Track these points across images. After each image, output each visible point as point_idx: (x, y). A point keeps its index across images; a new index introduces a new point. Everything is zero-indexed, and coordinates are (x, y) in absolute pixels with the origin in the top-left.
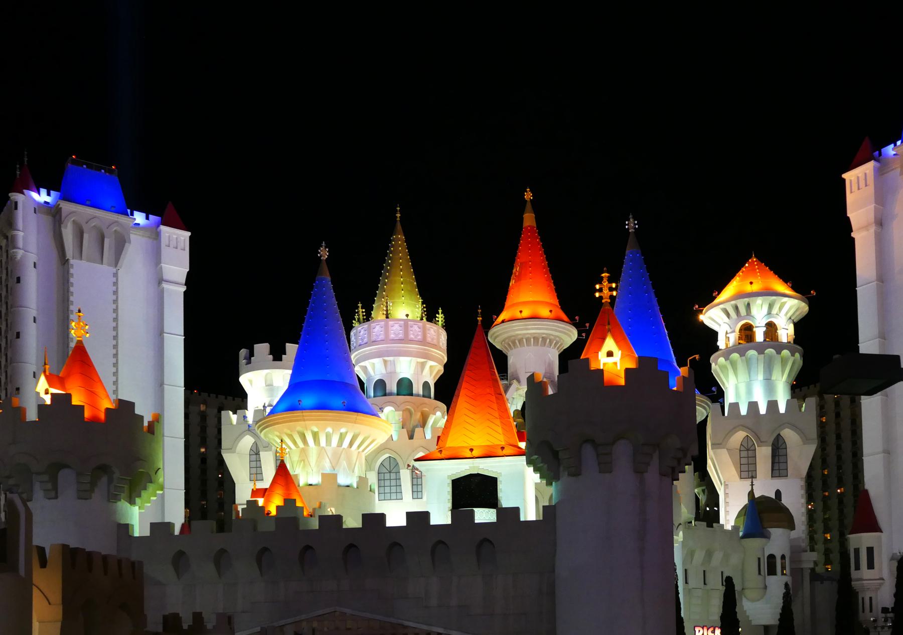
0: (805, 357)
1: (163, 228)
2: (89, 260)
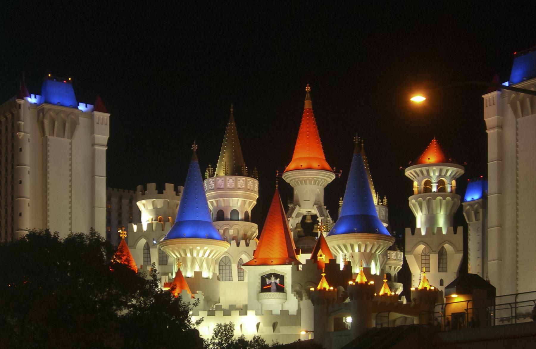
1: (96, 113)
2: (58, 136)
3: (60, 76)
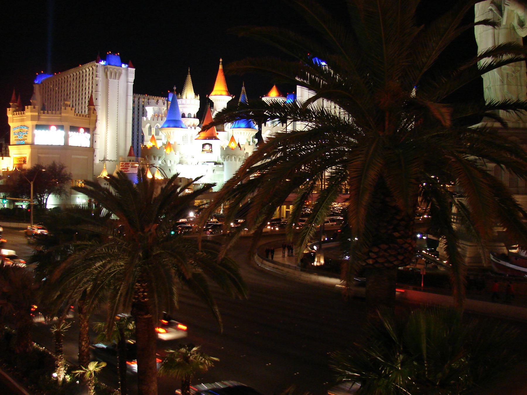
3: (114, 52)
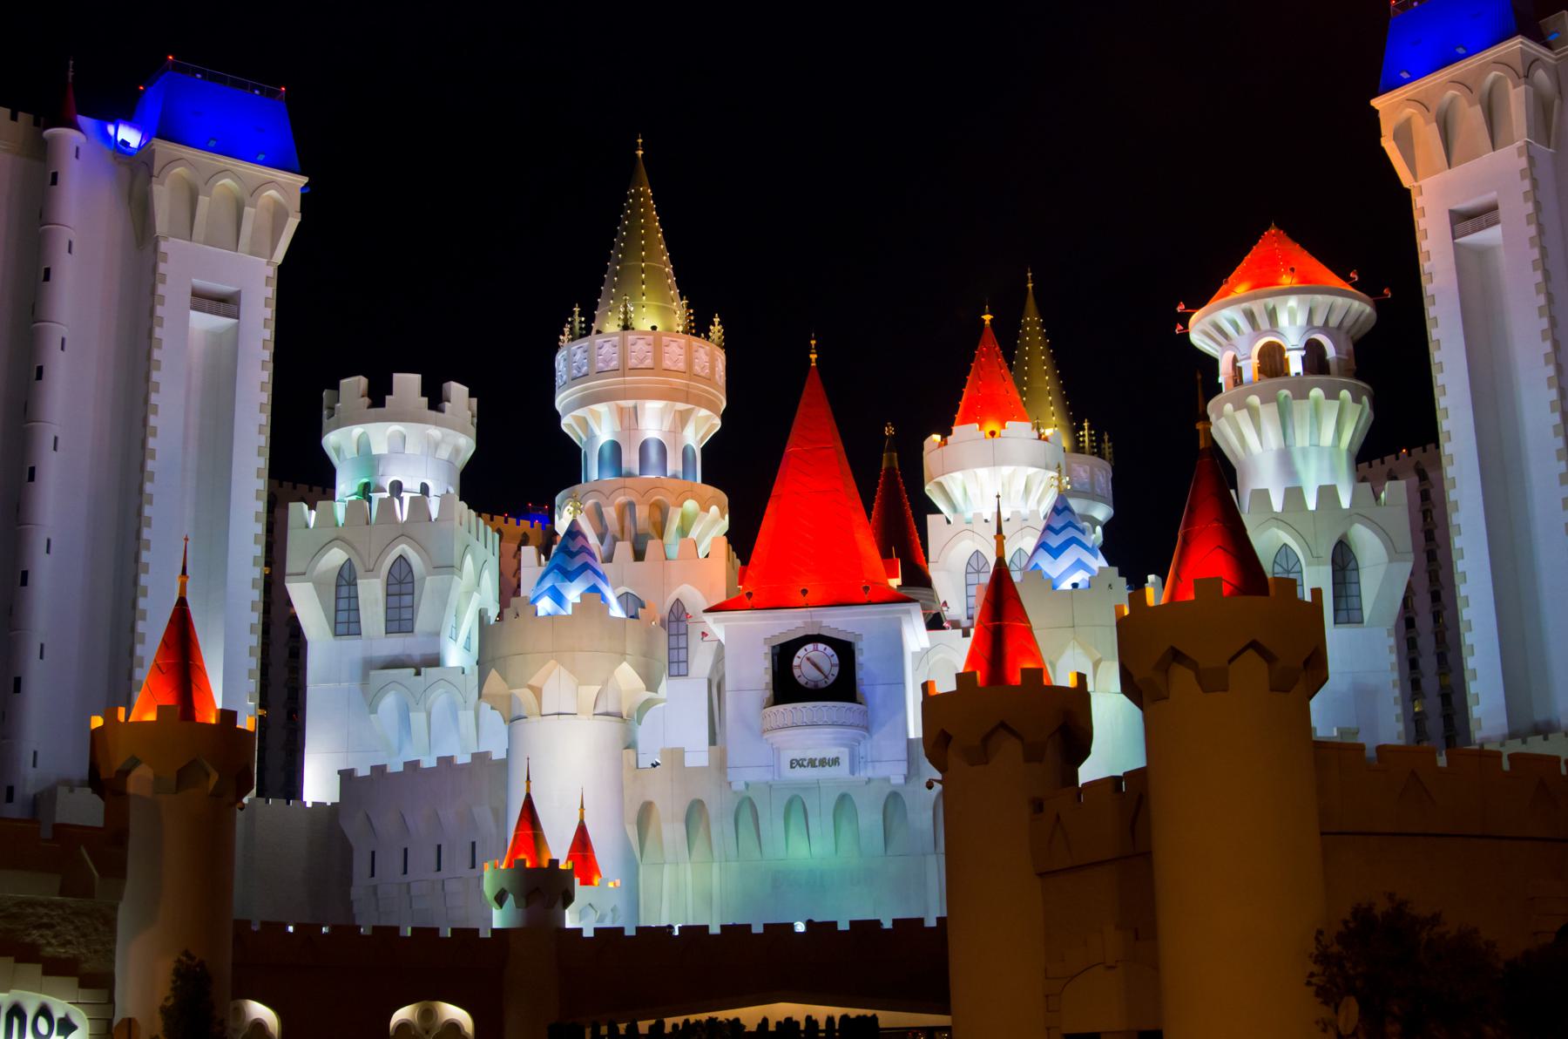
0: (1376, 405)
